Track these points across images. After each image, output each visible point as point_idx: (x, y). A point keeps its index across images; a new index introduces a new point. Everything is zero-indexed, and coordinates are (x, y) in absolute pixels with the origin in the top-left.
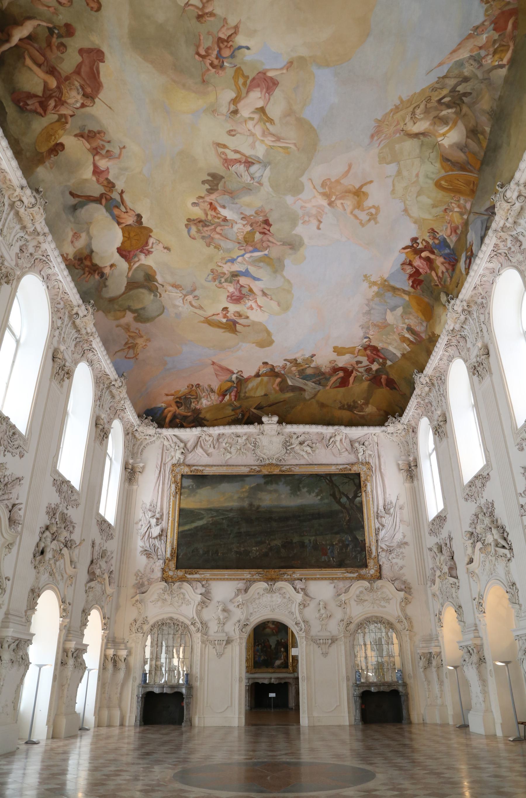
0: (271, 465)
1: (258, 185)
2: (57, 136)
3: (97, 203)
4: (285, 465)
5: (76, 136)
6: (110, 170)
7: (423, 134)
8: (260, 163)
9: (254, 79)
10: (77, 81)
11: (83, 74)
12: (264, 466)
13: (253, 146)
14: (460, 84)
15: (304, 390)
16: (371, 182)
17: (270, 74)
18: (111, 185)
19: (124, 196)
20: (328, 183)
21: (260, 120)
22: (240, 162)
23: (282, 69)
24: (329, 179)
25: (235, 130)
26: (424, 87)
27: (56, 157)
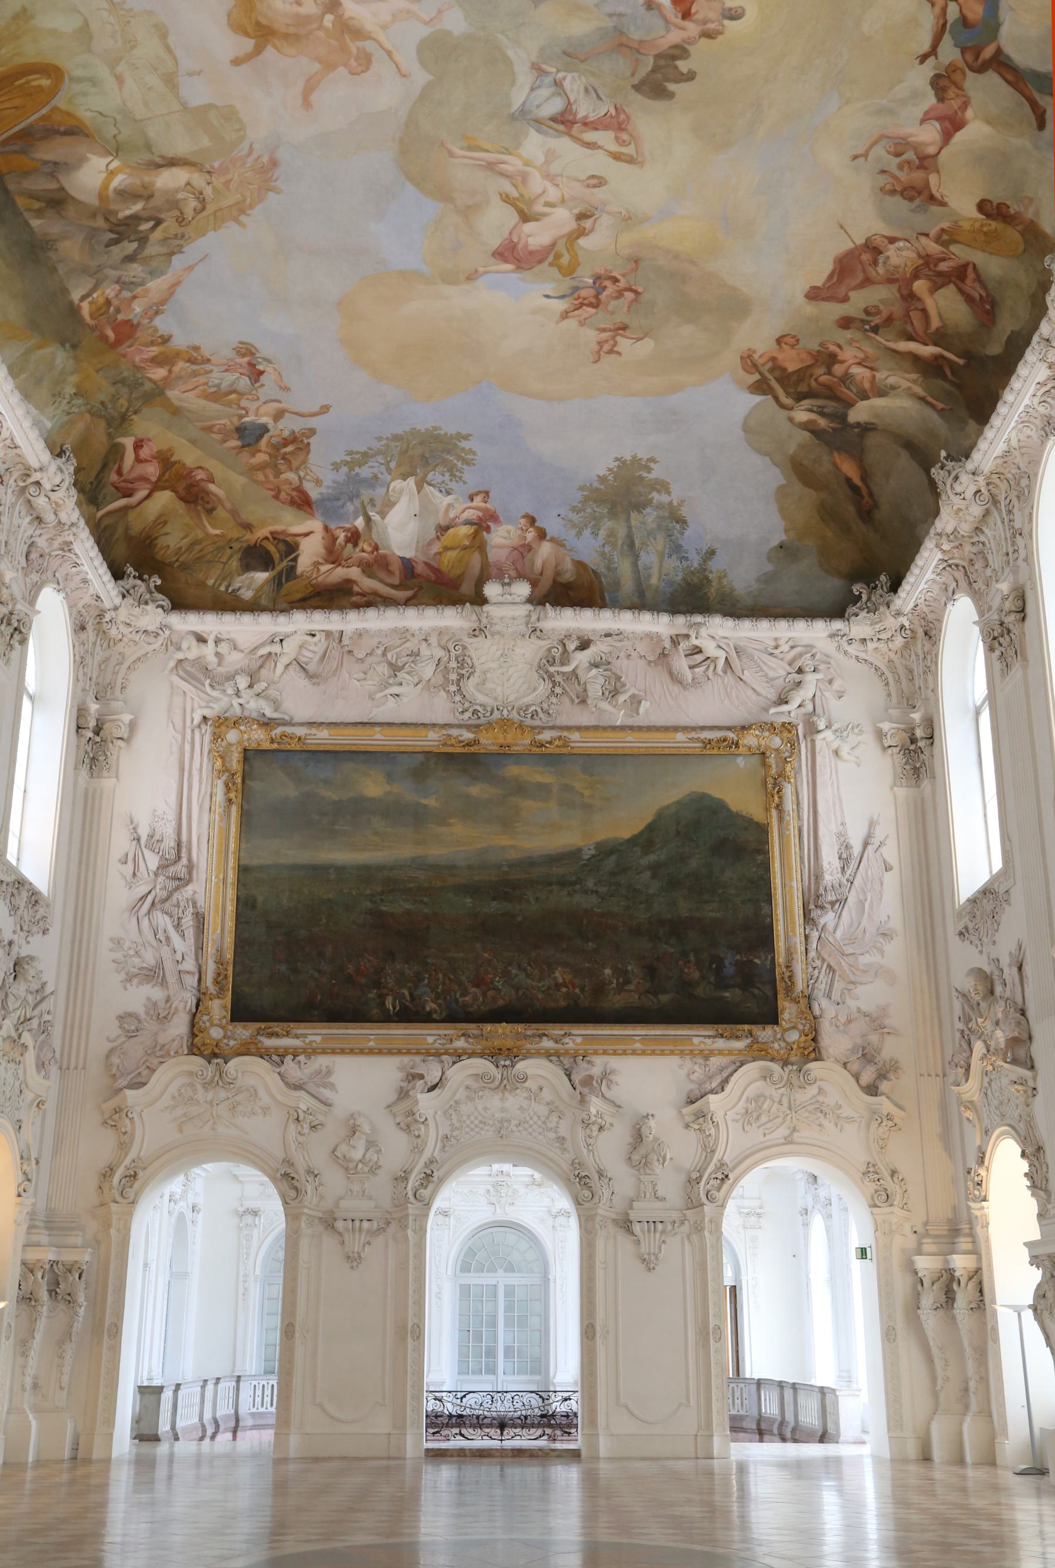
1: (544, 66)
2: (977, 225)
3: (1008, 57)
5: (943, 204)
6: (921, 115)
7: (158, 166)
8: (536, 121)
9: (540, 262)
10: (877, 272)
11: (860, 277)
13: (551, 156)
14: (135, 251)
16: (237, 62)
17: (510, 267)
18: (941, 84)
19: (926, 47)
20: (353, 63)
21: (531, 202)
22: (585, 124)
23: (485, 273)
24: (352, 73)
25: (588, 186)
26: (203, 239)
27: (1008, 203)
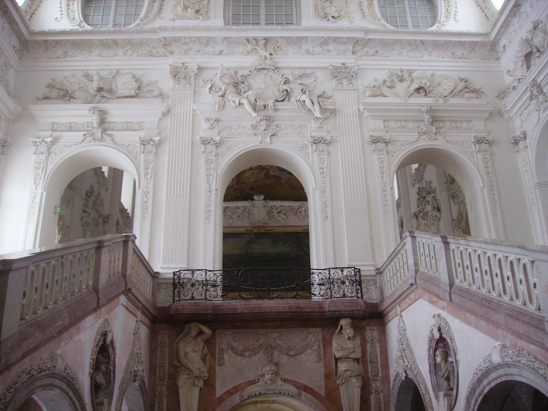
0: (259, 226)
4: (269, 227)
12: (255, 227)
15: (281, 178)
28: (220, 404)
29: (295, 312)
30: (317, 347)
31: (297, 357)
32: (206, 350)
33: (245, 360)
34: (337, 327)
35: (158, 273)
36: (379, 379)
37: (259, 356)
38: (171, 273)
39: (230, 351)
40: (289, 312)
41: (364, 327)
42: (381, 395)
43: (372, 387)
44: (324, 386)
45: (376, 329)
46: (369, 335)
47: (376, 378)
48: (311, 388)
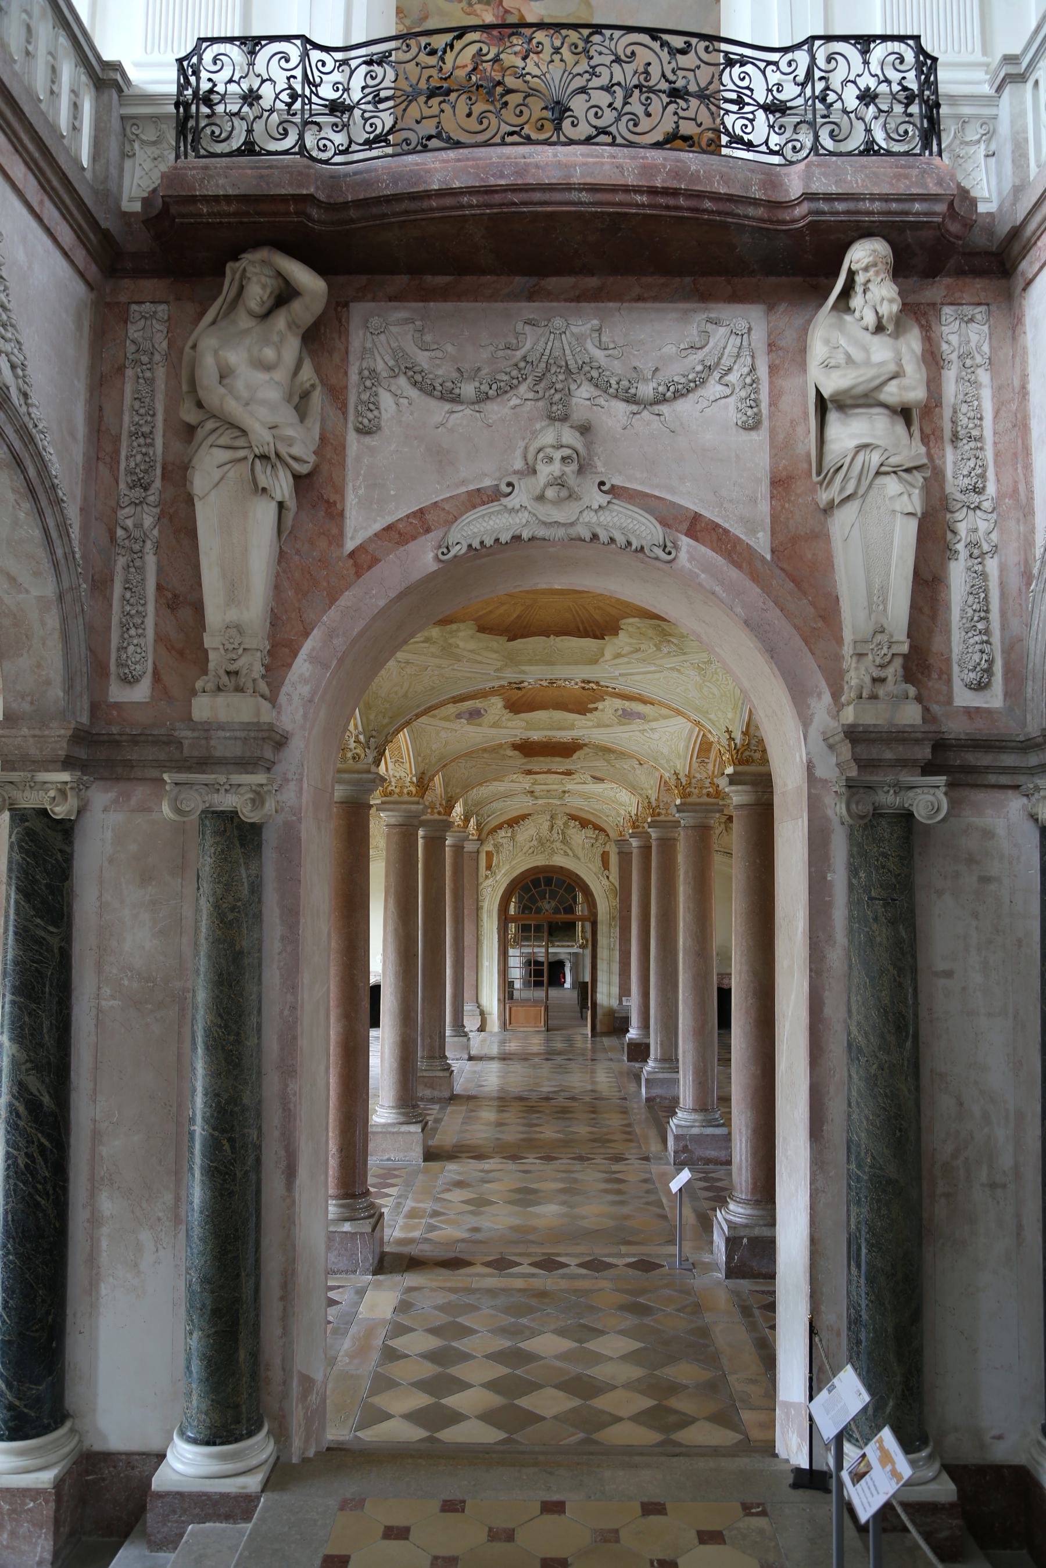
28: (358, 575)
29: (666, 192)
30: (746, 370)
31: (664, 408)
32: (307, 373)
33: (463, 415)
34: (837, 275)
35: (116, 67)
36: (987, 505)
37: (515, 401)
38: (168, 65)
39: (402, 381)
40: (637, 190)
41: (934, 304)
42: (992, 566)
43: (954, 533)
44: (768, 520)
45: (979, 317)
46: (954, 339)
47: (975, 499)
48: (718, 526)
